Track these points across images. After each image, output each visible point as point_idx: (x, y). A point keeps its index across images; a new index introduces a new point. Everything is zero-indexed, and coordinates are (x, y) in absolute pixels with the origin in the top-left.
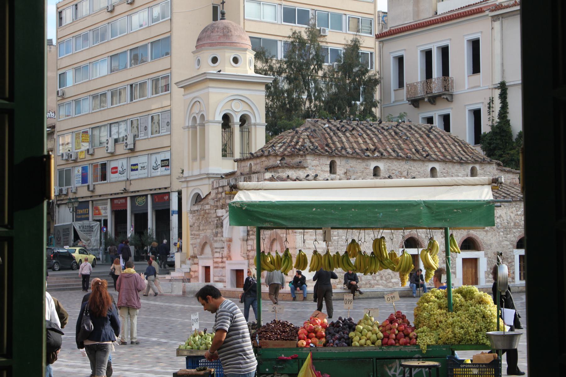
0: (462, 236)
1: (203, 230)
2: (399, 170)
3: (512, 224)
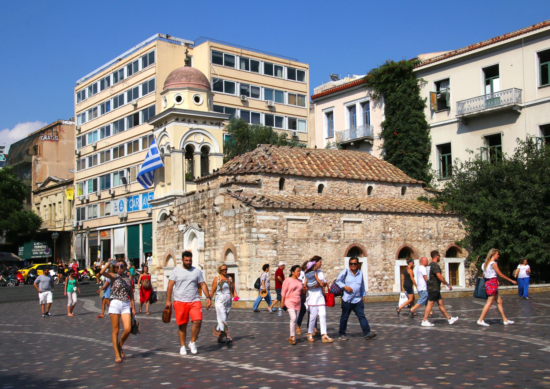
0: (400, 245)
2: (341, 188)
3: (442, 235)
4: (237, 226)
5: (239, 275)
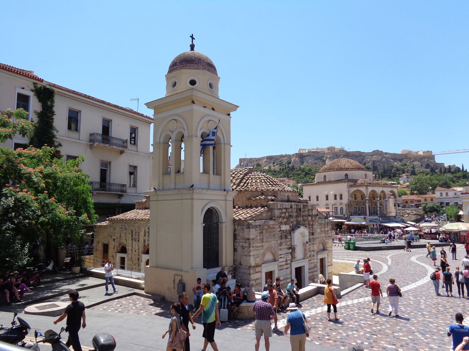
1: (267, 242)
4: (326, 229)
5: (328, 258)
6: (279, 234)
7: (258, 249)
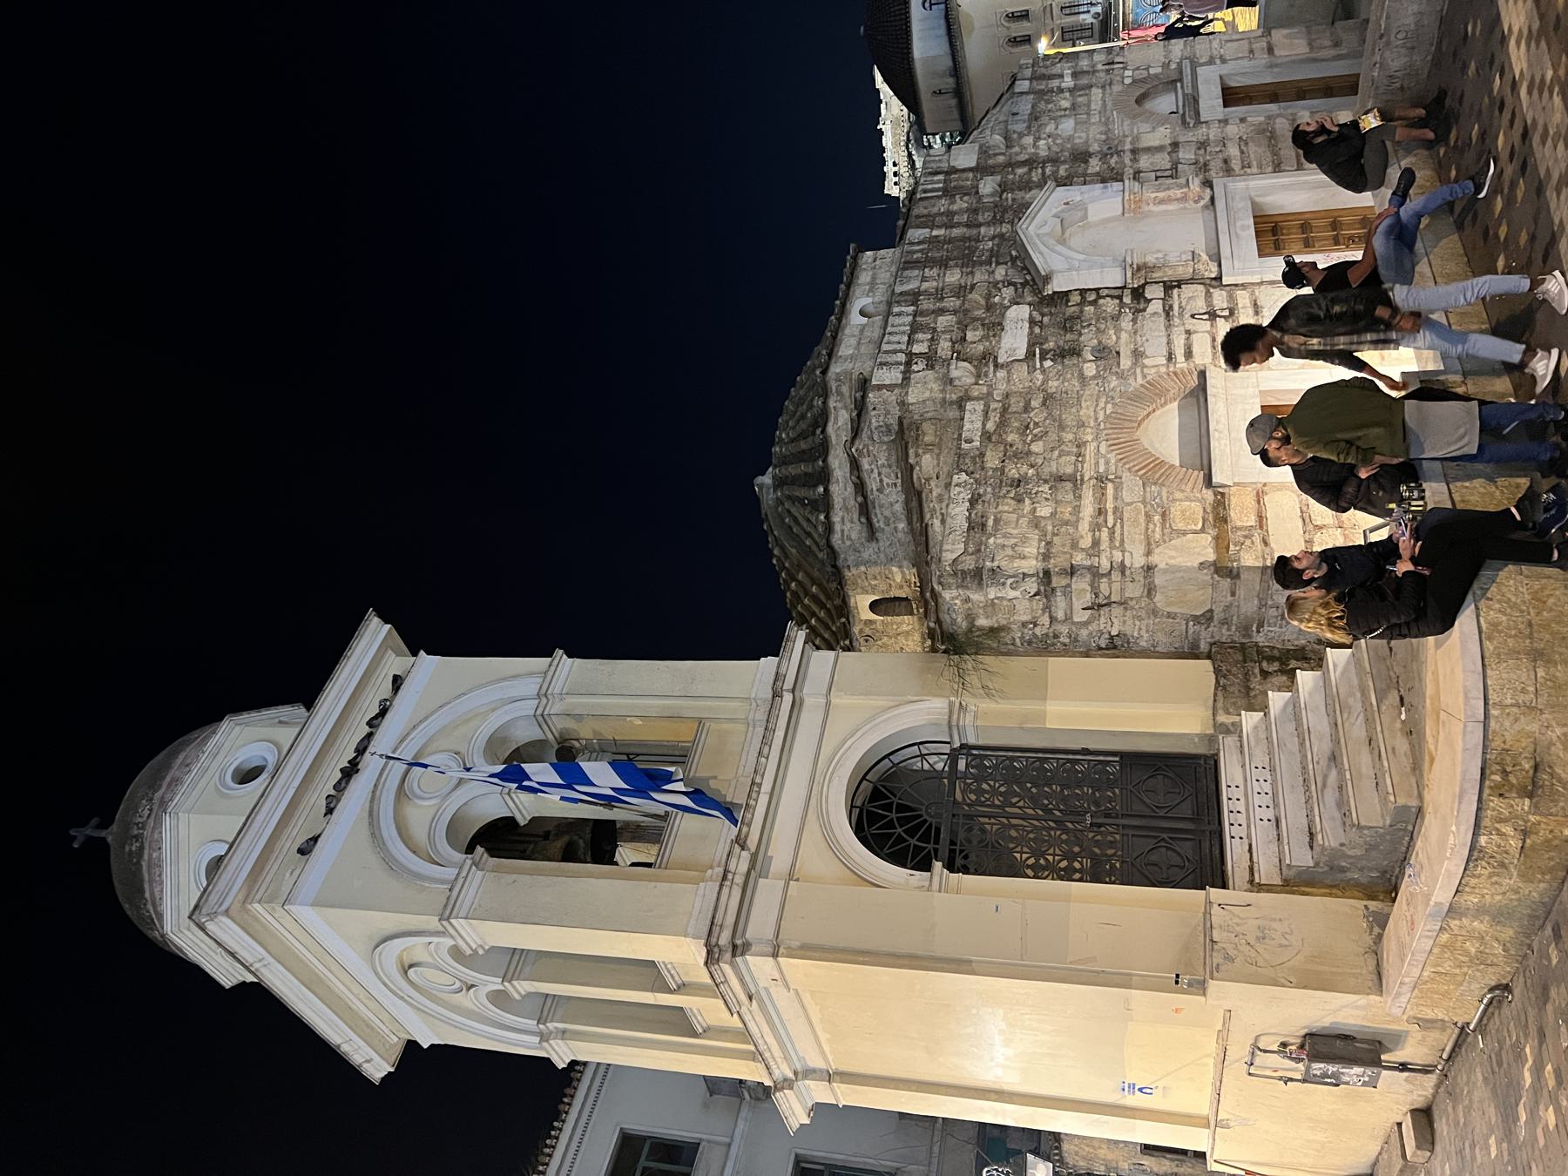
4: (1068, 82)
5: (1224, 61)
6: (1043, 371)
7: (1116, 509)
